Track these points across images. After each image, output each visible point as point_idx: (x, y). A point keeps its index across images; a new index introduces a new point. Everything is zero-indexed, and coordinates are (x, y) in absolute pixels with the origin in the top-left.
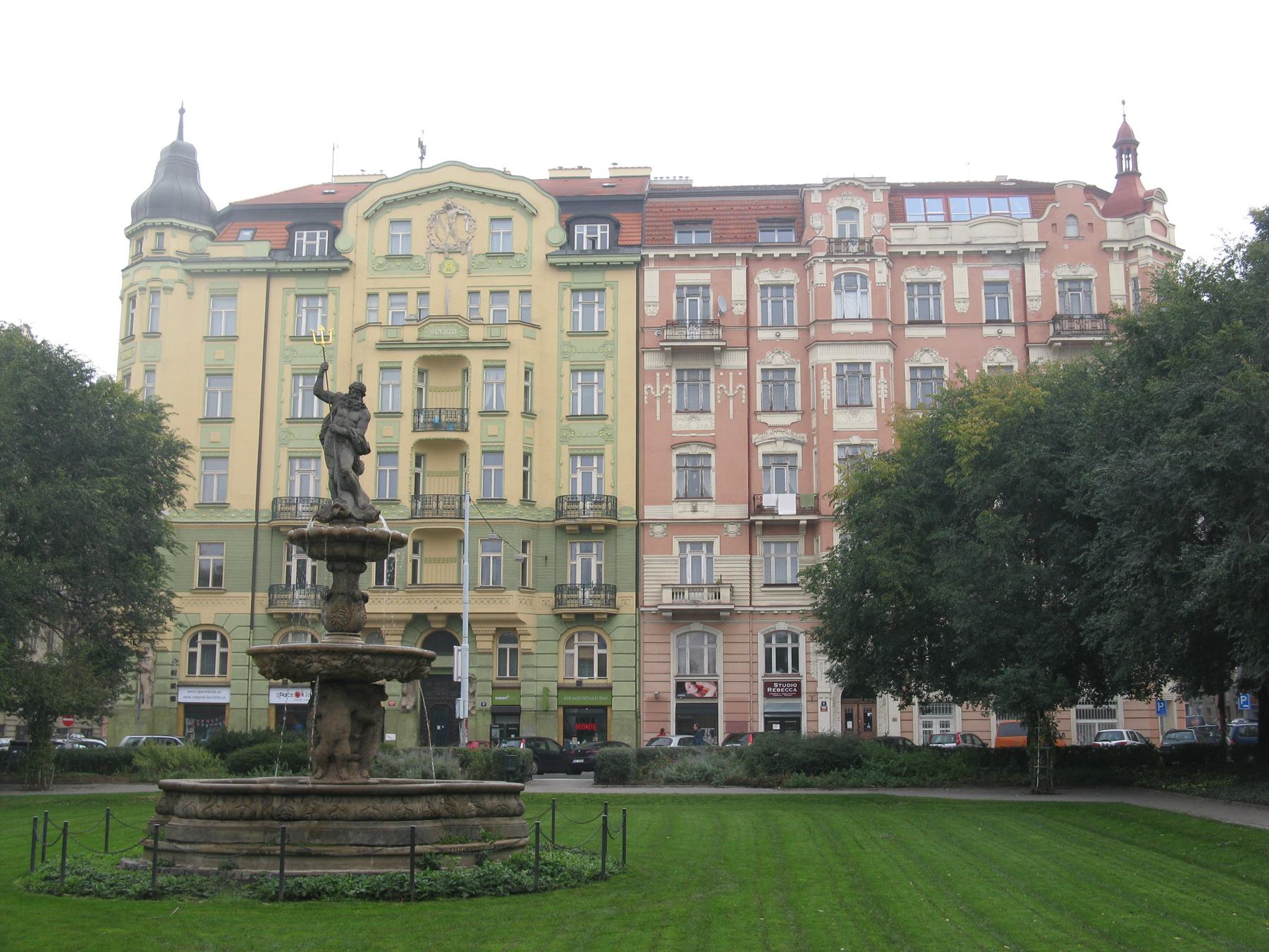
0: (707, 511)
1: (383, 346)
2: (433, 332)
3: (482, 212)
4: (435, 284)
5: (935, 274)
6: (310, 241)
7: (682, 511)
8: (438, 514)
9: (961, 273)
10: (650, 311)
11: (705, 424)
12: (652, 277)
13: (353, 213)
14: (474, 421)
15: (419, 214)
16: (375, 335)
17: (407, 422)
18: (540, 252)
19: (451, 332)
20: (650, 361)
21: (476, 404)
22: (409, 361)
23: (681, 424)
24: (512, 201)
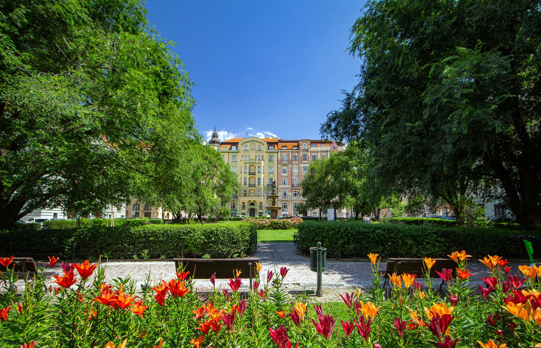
0: (286, 186)
1: (244, 163)
2: (251, 161)
3: (257, 144)
4: (251, 154)
5: (316, 154)
6: (234, 148)
7: (283, 186)
8: (252, 187)
9: (319, 154)
10: (279, 159)
11: (286, 174)
12: (279, 154)
13: (239, 144)
14: (256, 174)
15: (248, 144)
16: (244, 162)
17: (248, 174)
18: (265, 150)
19: (253, 161)
20: (279, 166)
21: (257, 172)
22: (248, 165)
23: (283, 174)
24: (261, 143)
